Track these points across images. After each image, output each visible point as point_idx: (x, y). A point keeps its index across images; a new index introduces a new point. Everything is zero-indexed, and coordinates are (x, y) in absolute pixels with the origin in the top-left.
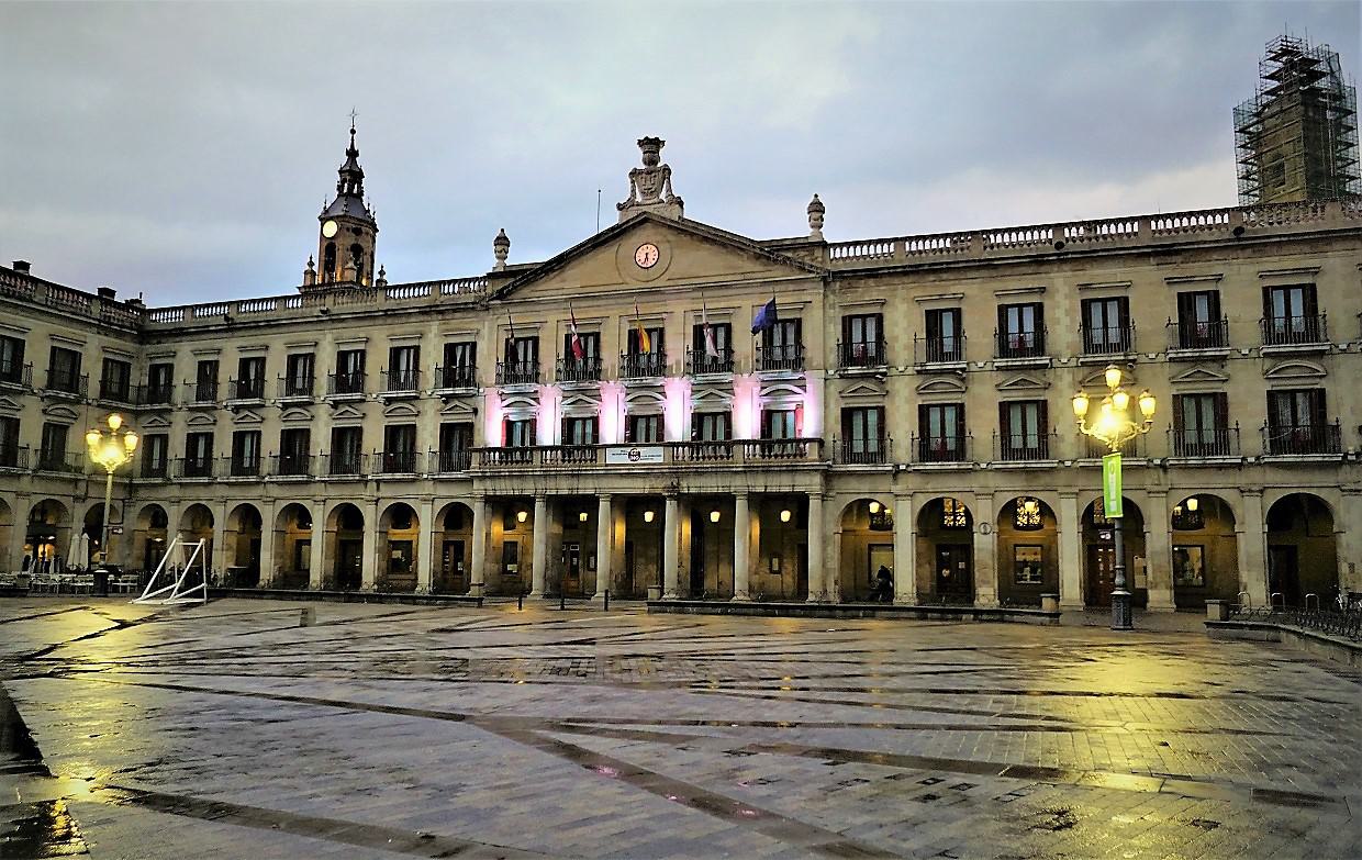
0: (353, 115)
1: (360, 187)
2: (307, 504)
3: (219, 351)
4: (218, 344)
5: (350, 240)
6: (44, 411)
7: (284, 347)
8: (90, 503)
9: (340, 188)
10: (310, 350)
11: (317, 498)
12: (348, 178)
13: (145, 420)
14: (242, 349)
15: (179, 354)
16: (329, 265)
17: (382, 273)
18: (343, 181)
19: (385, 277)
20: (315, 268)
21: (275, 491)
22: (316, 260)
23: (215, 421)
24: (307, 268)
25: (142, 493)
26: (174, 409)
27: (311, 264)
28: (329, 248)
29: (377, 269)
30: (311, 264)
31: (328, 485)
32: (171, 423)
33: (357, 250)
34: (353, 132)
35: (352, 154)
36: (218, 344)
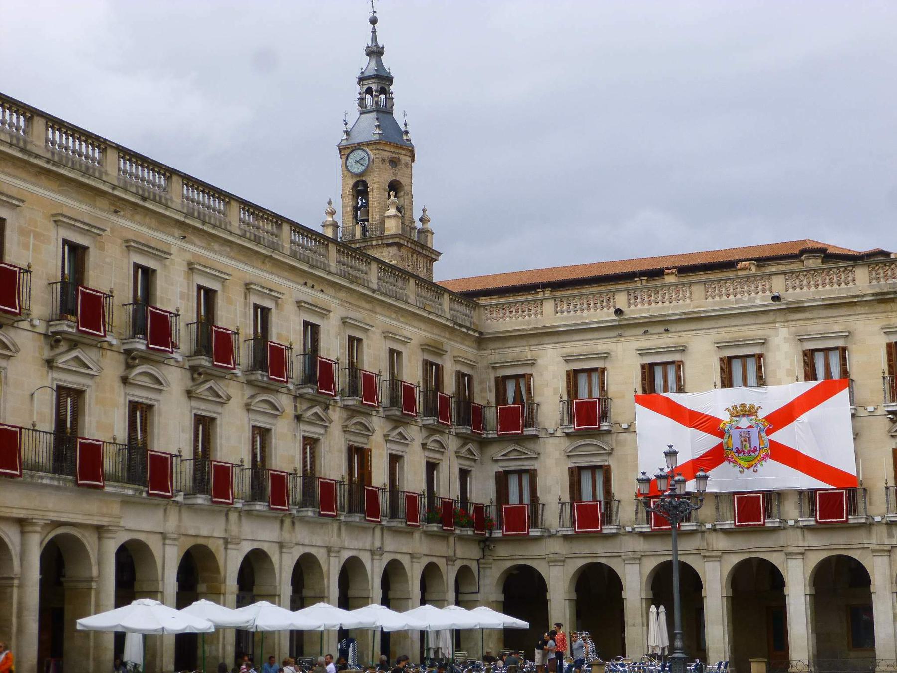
1: (389, 99)
2: (775, 559)
3: (606, 356)
4: (602, 347)
6: (424, 446)
7: (713, 348)
8: (459, 564)
9: (362, 100)
10: (756, 351)
12: (374, 87)
13: (497, 451)
14: (643, 353)
16: (360, 212)
18: (369, 91)
20: (338, 218)
21: (721, 543)
23: (612, 449)
25: (502, 551)
26: (542, 434)
28: (360, 190)
29: (417, 215)
31: (806, 532)
32: (539, 454)
33: (394, 187)
34: (374, 21)
35: (376, 52)
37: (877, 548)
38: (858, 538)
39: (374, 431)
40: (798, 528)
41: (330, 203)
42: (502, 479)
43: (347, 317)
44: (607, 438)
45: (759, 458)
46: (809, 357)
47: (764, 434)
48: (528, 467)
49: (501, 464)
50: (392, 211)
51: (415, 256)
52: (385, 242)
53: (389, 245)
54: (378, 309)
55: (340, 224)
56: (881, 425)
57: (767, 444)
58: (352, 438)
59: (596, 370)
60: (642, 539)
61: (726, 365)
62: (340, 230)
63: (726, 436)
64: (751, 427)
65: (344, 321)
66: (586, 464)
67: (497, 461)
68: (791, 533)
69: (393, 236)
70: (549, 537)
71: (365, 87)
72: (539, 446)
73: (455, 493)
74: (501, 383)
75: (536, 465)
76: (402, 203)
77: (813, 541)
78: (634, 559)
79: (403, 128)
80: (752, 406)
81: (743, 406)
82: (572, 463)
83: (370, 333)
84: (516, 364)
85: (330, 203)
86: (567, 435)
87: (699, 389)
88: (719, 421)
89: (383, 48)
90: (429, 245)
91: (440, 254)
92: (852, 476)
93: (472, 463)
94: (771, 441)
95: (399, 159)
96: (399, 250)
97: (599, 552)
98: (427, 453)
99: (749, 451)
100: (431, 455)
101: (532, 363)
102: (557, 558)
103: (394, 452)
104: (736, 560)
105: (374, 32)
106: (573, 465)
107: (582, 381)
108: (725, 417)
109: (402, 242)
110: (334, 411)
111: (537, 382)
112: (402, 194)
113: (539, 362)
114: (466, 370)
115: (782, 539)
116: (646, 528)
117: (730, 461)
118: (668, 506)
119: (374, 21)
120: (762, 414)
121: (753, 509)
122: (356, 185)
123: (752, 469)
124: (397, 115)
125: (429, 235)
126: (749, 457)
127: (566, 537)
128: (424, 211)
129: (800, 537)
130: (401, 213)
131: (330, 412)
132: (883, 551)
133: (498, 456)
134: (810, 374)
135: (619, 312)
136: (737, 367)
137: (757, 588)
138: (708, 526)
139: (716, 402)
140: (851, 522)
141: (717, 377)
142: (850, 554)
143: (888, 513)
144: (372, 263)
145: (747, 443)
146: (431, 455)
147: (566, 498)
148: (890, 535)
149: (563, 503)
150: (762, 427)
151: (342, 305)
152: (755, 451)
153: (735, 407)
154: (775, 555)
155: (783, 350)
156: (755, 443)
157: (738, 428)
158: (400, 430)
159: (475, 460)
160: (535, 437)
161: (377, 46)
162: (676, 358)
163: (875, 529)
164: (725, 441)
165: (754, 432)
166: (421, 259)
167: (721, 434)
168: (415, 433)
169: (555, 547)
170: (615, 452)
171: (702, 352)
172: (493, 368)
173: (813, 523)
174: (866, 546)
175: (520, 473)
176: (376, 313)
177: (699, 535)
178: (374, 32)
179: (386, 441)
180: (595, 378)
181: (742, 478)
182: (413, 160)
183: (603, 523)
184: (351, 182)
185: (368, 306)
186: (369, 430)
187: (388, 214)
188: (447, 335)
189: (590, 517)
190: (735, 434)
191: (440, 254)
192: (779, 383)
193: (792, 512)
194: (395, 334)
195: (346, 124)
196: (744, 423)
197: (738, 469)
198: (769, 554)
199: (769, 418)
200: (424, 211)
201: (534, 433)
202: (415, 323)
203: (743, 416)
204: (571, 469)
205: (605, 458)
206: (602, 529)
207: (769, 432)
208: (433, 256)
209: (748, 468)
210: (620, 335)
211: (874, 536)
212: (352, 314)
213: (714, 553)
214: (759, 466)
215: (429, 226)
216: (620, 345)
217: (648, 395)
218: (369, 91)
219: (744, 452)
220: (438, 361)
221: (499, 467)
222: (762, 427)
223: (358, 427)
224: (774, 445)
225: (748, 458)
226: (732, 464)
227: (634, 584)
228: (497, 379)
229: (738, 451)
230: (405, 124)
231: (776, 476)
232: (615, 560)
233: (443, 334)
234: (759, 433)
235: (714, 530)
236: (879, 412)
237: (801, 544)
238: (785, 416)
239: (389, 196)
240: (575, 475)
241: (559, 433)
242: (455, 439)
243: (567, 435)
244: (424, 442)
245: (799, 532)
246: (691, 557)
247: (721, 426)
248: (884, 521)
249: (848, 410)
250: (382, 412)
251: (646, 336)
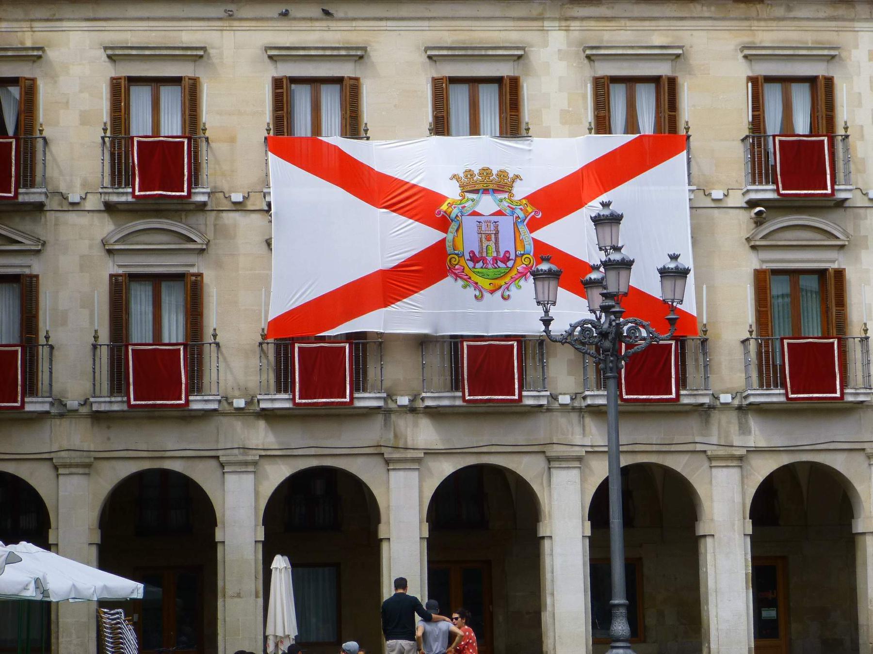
4: (190, 35)
11: (557, 451)
14: (276, 55)
21: (424, 434)
26: (53, 204)
31: (588, 420)
32: (44, 244)
36: (190, 35)
37: (721, 452)
38: (686, 432)
40: (574, 409)
44: (199, 219)
45: (514, 273)
46: (602, 87)
47: (523, 229)
48: (17, 271)
56: (735, 226)
57: (530, 247)
59: (176, 81)
60: (262, 424)
61: (441, 91)
63: (453, 227)
64: (499, 213)
66: (173, 270)
68: (562, 420)
70: (61, 416)
72: (45, 228)
75: (36, 267)
77: (758, 434)
78: (246, 463)
80: (502, 174)
81: (486, 172)
82: (112, 267)
86: (110, 208)
87: (388, 134)
88: (442, 199)
92: (693, 316)
94: (535, 241)
97: (169, 448)
99: (495, 260)
101: (35, 56)
102: (76, 458)
104: (446, 468)
106: (120, 271)
107: (141, 99)
108: (451, 191)
111: (44, 94)
113: (52, 54)
115: (540, 430)
116: (282, 402)
117: (457, 276)
118: (318, 359)
120: (521, 191)
121: (489, 370)
123: (498, 293)
126: (492, 269)
127: (98, 418)
129: (578, 429)
132: (732, 457)
134: (602, 125)
136: (459, 99)
137: (484, 520)
138: (404, 401)
139: (431, 162)
140: (685, 400)
141: (427, 115)
142: (670, 462)
143: (586, 387)
145: (492, 244)
147: (104, 337)
148: (744, 430)
150: (521, 215)
152: (506, 259)
153: (469, 173)
154: (526, 459)
155: (555, 69)
156: (507, 244)
157: (475, 214)
160: (39, 208)
162: (345, 70)
163: (715, 416)
164: (450, 237)
165: (506, 225)
167: (443, 223)
169: (75, 437)
170: (212, 250)
171: (397, 61)
173: (459, 402)
174: (699, 447)
177: (380, 418)
180: (171, 99)
181: (479, 309)
183: (190, 391)
189: (156, 377)
190: (469, 224)
192: (546, 134)
193: (564, 379)
196: (487, 204)
197: (471, 292)
198: (516, 458)
199: (532, 199)
201: (42, 198)
203: (486, 191)
206: (187, 401)
207: (534, 225)
209: (492, 292)
210: (231, 17)
211: (714, 429)
213: (410, 454)
214: (513, 288)
217: (282, 139)
219: (484, 260)
222: (521, 215)
224: (543, 251)
225: (491, 272)
226: (460, 282)
227: (240, 508)
229: (474, 259)
231: (516, 312)
232: (201, 465)
234: (515, 225)
235: (412, 410)
236: (730, 202)
237: (578, 439)
238: (556, 201)
240: (119, 290)
241: (93, 202)
243: (110, 208)
245: (574, 416)
246: (360, 461)
247: (444, 207)
248: (736, 402)
249: (683, 192)
251: (284, 24)
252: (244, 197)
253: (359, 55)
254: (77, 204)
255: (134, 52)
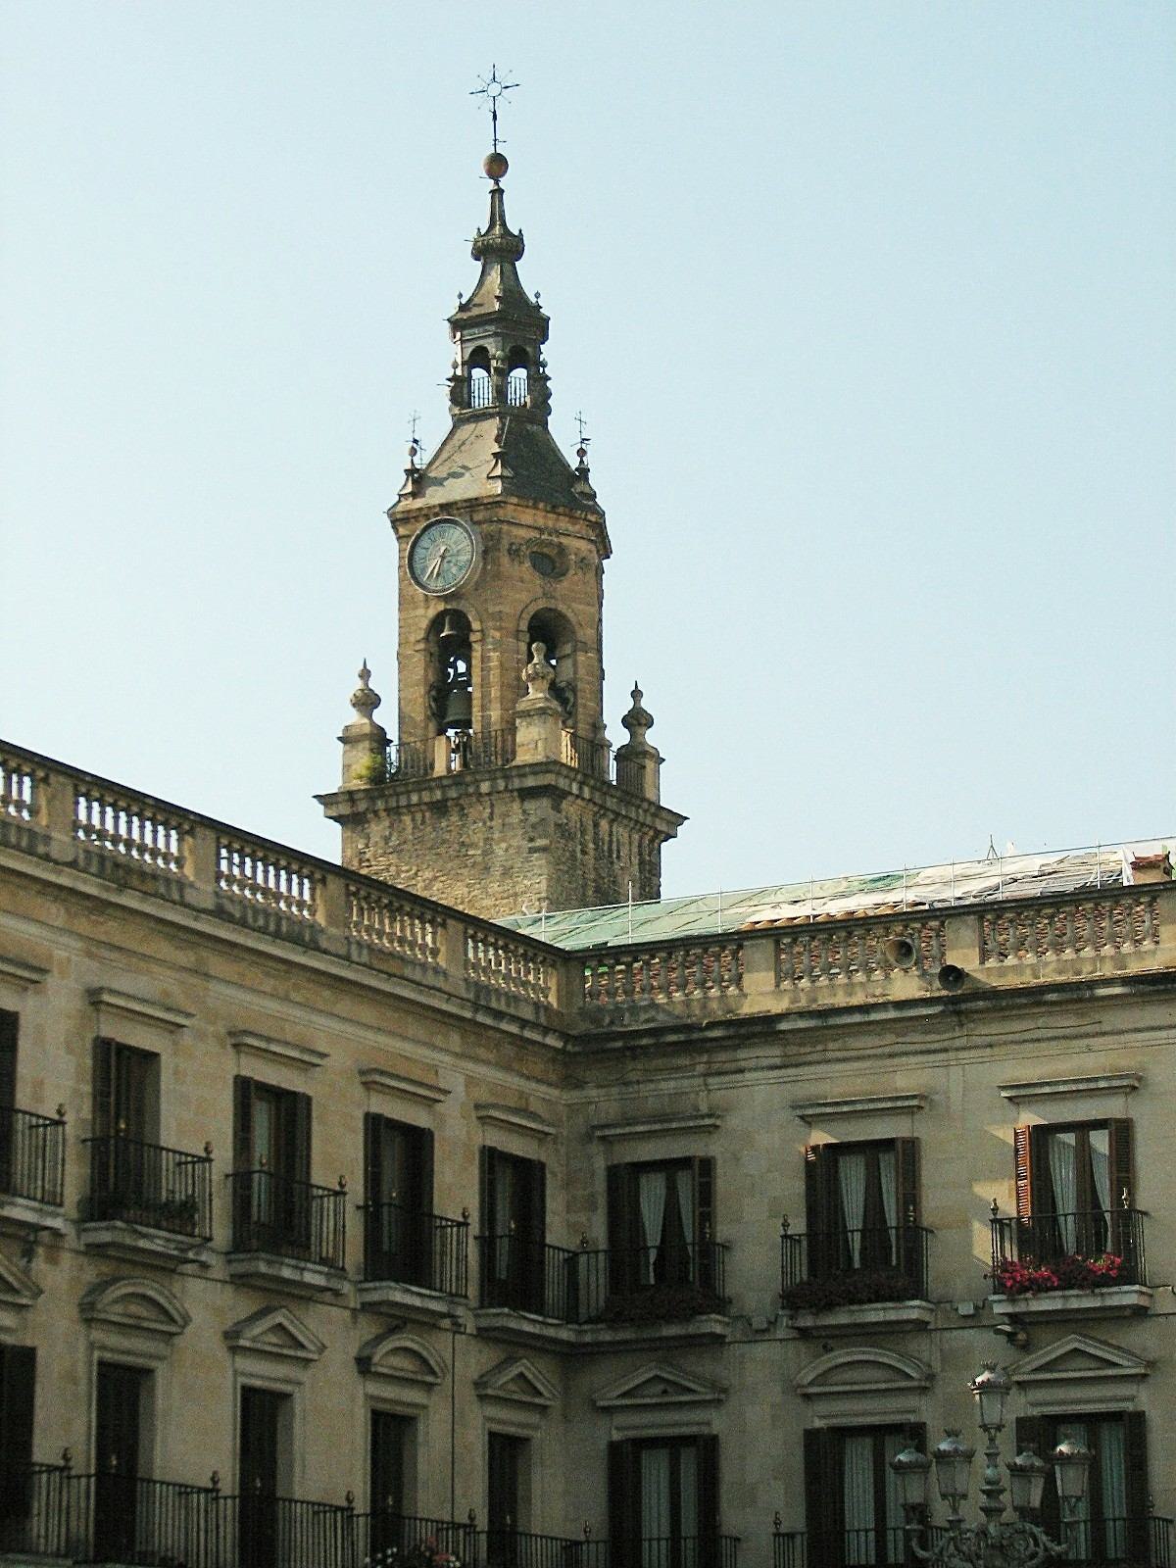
0: (495, 88)
1: (539, 383)
3: (913, 1106)
4: (907, 1078)
5: (524, 591)
6: (364, 1365)
9: (460, 391)
12: (493, 347)
13: (610, 1382)
15: (733, 1122)
16: (445, 701)
17: (637, 720)
18: (479, 358)
19: (651, 737)
20: (387, 717)
22: (386, 684)
23: (931, 1377)
24: (353, 717)
27: (367, 702)
28: (446, 639)
29: (615, 707)
30: (367, 702)
34: (497, 165)
35: (500, 249)
39: (187, 1320)
41: (365, 674)
42: (623, 1465)
43: (101, 989)
49: (620, 1419)
50: (536, 695)
51: (604, 824)
52: (516, 783)
53: (527, 794)
54: (217, 964)
55: (393, 734)
58: (114, 1340)
59: (888, 1144)
62: (392, 751)
65: (94, 998)
67: (608, 1410)
69: (536, 768)
71: (470, 348)
73: (474, 1498)
74: (623, 1182)
75: (718, 1423)
76: (566, 671)
79: (574, 462)
83: (187, 1039)
84: (665, 1123)
85: (365, 674)
89: (520, 238)
90: (650, 795)
91: (681, 819)
93: (534, 1418)
95: (562, 550)
96: (557, 809)
98: (374, 1388)
100: (389, 1392)
101: (708, 1124)
103: (258, 1383)
105: (497, 193)
109: (562, 783)
110: (53, 1260)
112: (568, 649)
114: (516, 1146)
119: (497, 165)
122: (437, 623)
124: (563, 432)
125: (650, 764)
128: (636, 694)
130: (564, 702)
131: (39, 1264)
133: (610, 1397)
135: (952, 975)
144: (199, 831)
146: (389, 1392)
149: (791, 1536)
151: (90, 955)
158: (279, 1318)
159: (543, 1409)
160: (718, 1340)
161: (506, 232)
162: (1112, 1108)
166: (621, 832)
168: (333, 1332)
172: (603, 1138)
175: (674, 1444)
176: (207, 976)
178: (497, 193)
179: (234, 1350)
182: (606, 552)
184: (426, 614)
185: (186, 958)
186: (173, 1320)
187: (522, 706)
188: (455, 1041)
191: (681, 819)
194: (269, 1040)
195: (413, 452)
200: (636, 694)
202: (345, 1006)
204: (811, 1436)
205: (912, 1401)
208: (662, 826)
212: (124, 982)
215: (651, 737)
216: (956, 1073)
218: (479, 358)
220: (419, 1118)
221: (615, 1430)
223: (133, 1309)
228: (613, 1172)
230: (582, 453)
233: (438, 1040)
239: (530, 657)
240: (823, 1454)
242: (474, 1346)
244: (366, 1353)
250: (218, 1268)
252: (976, 1308)
253: (1132, 1086)
254: (764, 1331)
255: (829, 1110)
